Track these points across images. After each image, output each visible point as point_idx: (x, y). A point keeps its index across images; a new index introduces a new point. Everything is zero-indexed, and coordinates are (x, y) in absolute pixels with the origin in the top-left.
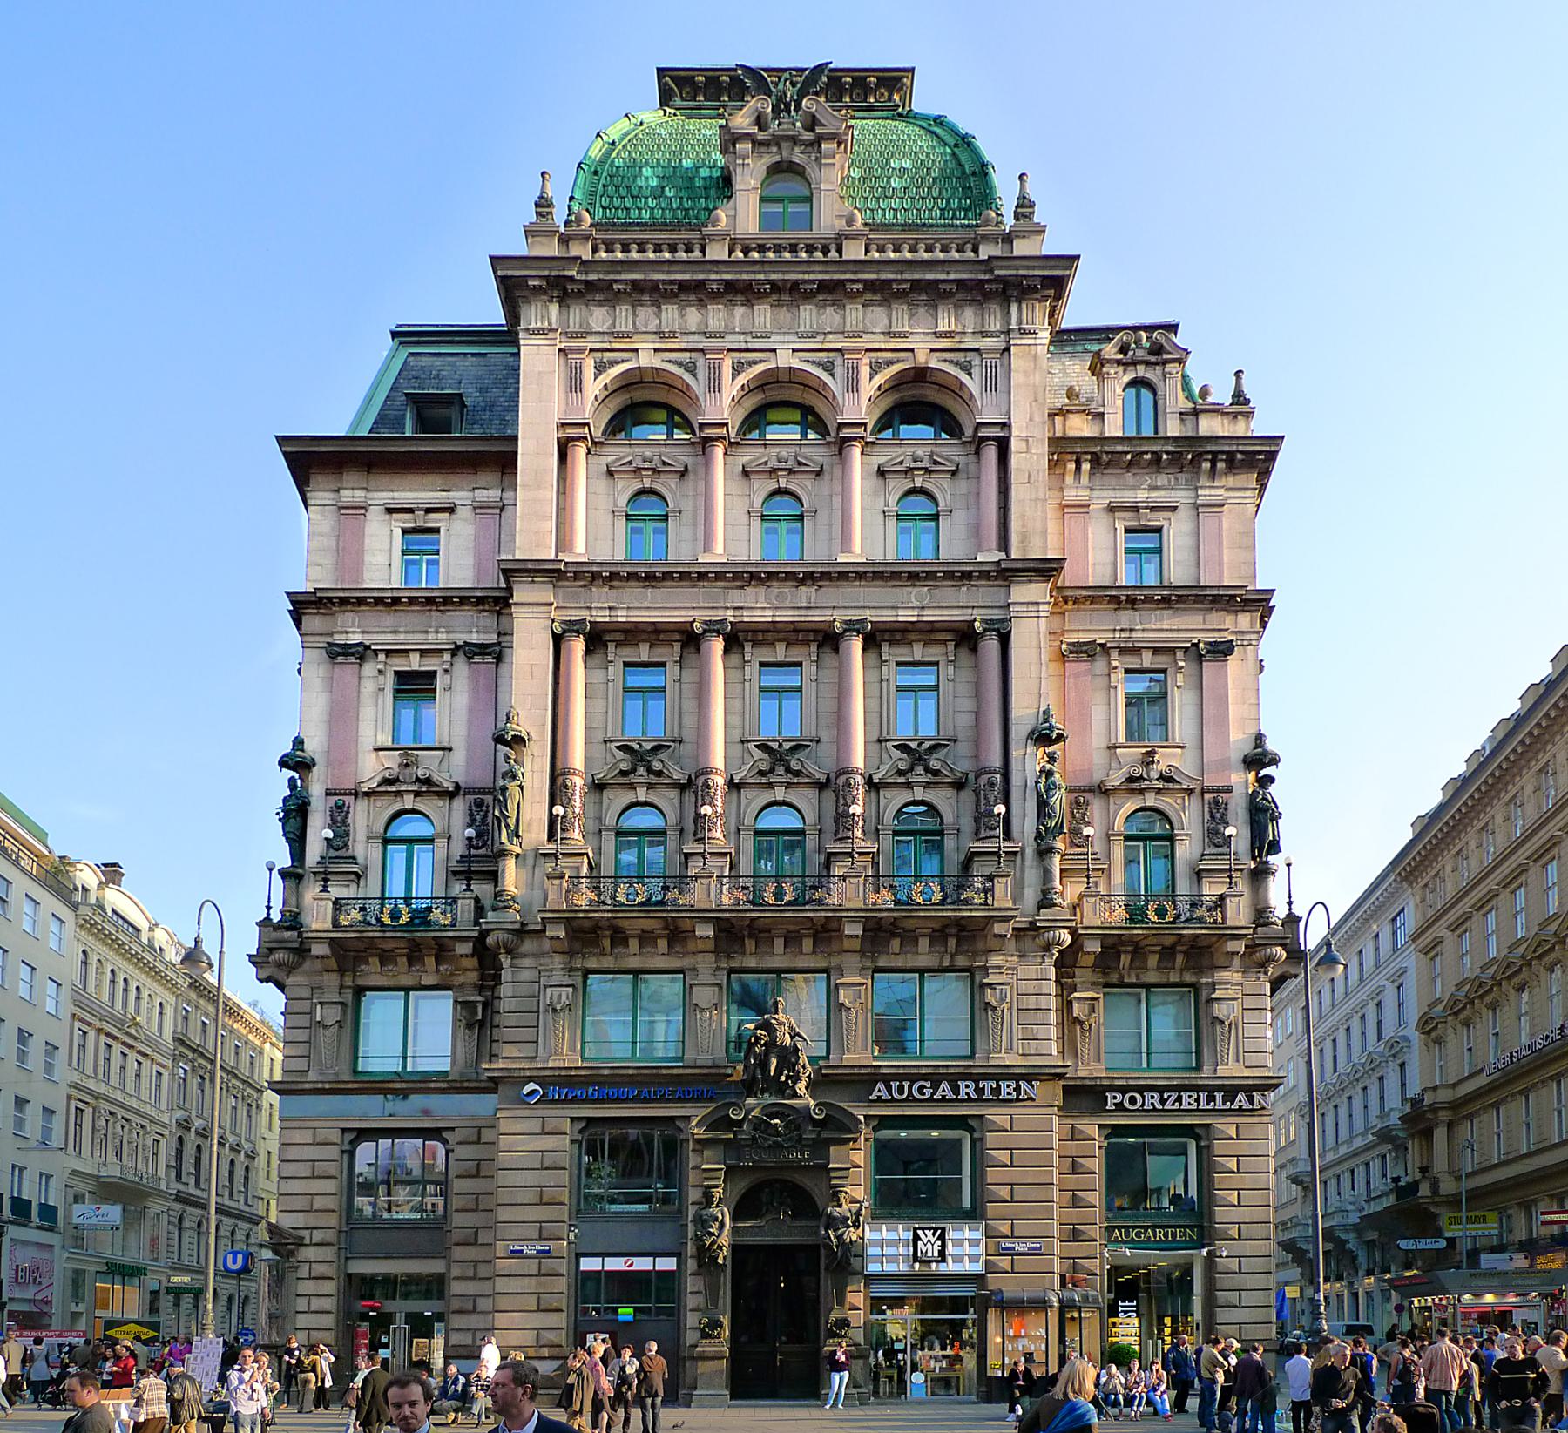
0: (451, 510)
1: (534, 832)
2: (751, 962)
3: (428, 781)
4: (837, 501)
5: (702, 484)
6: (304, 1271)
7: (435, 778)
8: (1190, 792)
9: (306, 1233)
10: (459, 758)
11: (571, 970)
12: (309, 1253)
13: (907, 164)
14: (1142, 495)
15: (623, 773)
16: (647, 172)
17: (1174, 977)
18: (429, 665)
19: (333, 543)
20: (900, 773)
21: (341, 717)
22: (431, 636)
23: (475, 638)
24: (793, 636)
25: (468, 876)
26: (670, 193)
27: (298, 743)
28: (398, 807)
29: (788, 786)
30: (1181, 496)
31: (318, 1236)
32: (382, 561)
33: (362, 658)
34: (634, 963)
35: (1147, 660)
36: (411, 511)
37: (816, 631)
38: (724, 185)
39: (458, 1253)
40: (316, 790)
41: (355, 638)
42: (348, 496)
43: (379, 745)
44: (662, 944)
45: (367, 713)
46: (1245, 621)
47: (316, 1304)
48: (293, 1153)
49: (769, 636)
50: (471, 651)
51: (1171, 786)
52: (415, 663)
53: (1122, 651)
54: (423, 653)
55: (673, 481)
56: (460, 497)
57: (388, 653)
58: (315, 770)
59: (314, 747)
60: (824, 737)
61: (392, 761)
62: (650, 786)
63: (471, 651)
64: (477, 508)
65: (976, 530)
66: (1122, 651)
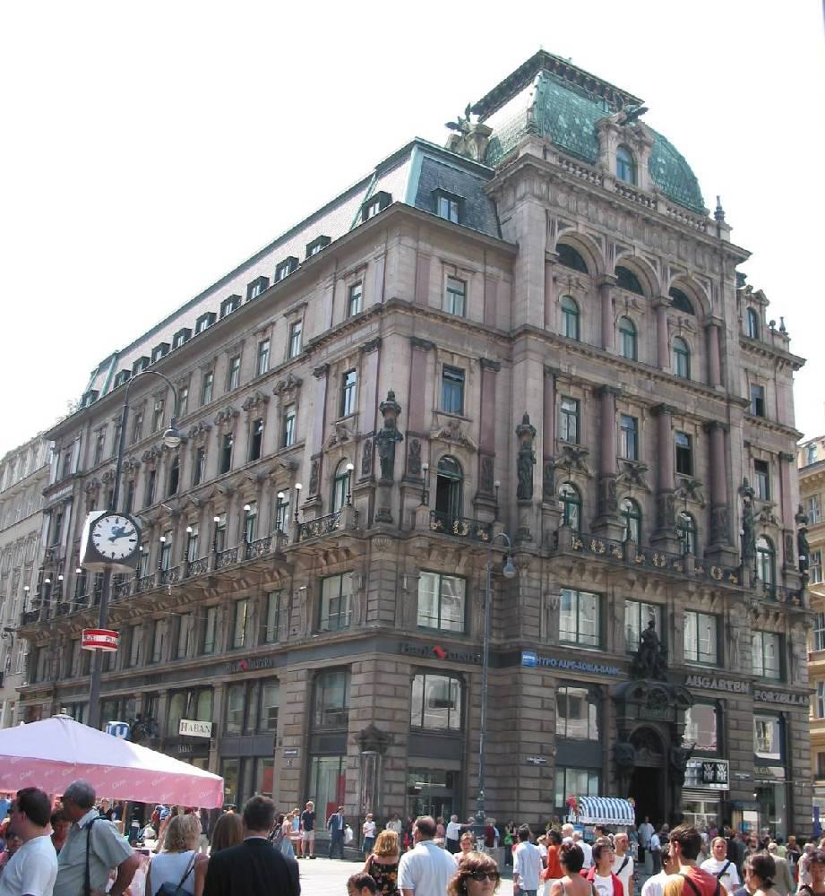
0: (475, 272)
1: (538, 495)
3: (464, 441)
4: (653, 332)
5: (598, 305)
6: (388, 764)
7: (469, 439)
9: (391, 735)
10: (475, 428)
12: (393, 751)
13: (664, 162)
14: (755, 368)
16: (561, 118)
17: (775, 630)
19: (412, 271)
20: (683, 495)
21: (414, 385)
23: (486, 355)
25: (496, 511)
26: (574, 135)
27: (391, 396)
30: (769, 373)
31: (398, 739)
32: (438, 293)
33: (427, 349)
34: (583, 585)
36: (455, 267)
38: (597, 140)
40: (401, 429)
41: (423, 335)
42: (424, 246)
45: (429, 387)
46: (792, 443)
47: (396, 788)
48: (384, 678)
49: (629, 400)
52: (456, 363)
56: (478, 266)
58: (400, 415)
59: (401, 399)
60: (648, 462)
61: (443, 420)
63: (483, 363)
64: (485, 273)
65: (708, 368)
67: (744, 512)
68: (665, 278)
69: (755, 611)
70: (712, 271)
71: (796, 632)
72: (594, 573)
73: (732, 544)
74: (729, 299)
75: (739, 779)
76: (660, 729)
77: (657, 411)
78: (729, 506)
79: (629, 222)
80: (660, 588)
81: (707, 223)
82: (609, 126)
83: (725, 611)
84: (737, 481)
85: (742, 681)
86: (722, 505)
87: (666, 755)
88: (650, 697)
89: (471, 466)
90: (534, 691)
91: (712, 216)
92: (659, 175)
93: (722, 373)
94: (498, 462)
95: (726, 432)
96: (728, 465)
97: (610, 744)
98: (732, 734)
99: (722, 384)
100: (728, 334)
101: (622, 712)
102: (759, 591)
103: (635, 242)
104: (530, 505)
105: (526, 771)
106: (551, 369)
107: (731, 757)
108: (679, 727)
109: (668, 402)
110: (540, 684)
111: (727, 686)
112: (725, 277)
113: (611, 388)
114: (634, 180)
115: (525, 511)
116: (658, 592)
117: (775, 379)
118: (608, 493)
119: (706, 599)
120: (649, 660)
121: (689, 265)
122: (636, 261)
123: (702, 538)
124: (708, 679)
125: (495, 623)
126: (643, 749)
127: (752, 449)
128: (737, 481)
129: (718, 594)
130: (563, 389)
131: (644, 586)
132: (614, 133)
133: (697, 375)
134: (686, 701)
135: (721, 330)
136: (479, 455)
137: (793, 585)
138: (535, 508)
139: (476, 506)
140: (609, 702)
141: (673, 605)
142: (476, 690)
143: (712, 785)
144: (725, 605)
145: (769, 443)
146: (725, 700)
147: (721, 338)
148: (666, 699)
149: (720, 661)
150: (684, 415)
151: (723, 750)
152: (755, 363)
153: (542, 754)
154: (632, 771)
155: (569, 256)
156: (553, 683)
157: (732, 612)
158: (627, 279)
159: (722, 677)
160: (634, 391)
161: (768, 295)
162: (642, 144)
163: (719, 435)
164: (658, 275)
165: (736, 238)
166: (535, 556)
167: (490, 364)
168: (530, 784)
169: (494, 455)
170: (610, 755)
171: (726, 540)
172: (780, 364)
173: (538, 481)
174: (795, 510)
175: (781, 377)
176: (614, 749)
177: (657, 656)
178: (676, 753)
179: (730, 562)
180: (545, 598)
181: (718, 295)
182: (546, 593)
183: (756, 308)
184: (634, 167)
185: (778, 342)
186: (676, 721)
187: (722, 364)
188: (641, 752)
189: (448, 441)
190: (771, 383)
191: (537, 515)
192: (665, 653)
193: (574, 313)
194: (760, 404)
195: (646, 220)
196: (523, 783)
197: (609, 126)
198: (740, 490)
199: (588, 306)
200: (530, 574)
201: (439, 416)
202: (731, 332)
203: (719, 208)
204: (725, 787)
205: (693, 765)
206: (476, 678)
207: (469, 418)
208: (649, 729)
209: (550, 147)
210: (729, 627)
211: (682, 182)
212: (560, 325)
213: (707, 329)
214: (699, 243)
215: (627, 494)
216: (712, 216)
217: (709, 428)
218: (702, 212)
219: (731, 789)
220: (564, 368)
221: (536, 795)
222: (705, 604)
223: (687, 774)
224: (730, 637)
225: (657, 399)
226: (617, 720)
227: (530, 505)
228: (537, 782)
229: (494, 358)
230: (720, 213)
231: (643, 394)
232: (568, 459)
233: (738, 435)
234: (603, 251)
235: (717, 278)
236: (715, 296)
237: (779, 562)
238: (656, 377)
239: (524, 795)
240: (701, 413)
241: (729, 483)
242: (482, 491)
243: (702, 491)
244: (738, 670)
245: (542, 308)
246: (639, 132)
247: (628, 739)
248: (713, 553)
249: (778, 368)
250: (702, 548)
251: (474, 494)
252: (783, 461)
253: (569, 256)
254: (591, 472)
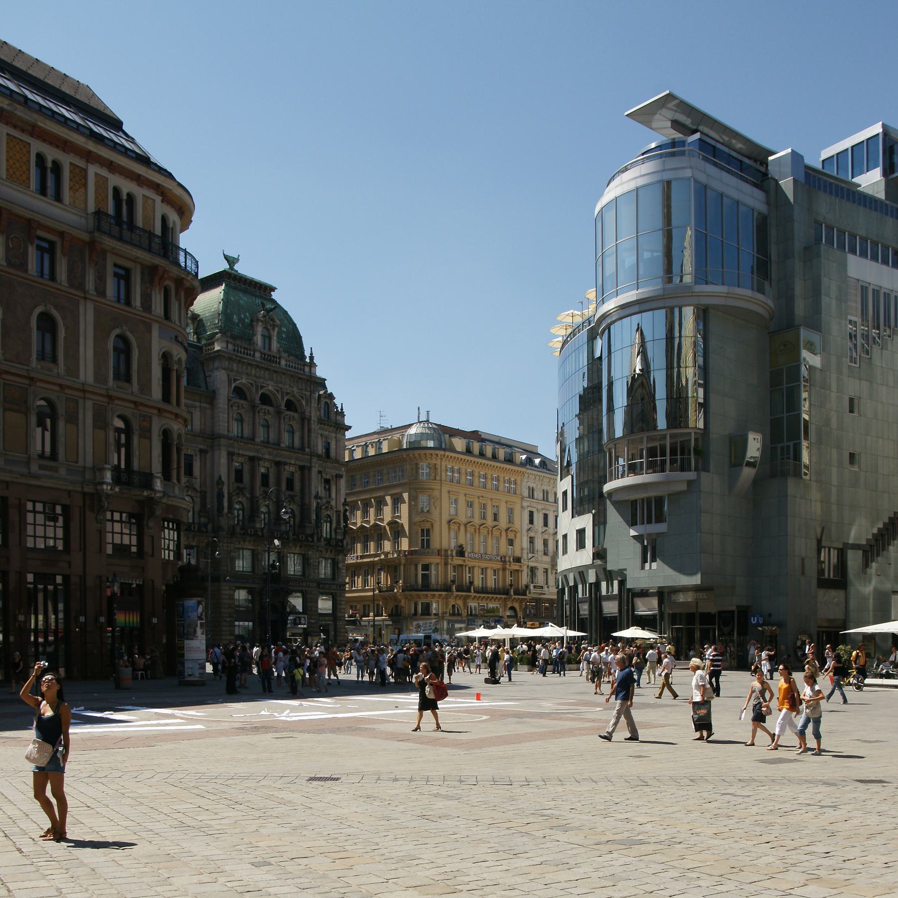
68: (283, 398)
70: (306, 390)
71: (340, 557)
72: (250, 542)
73: (310, 523)
74: (314, 404)
77: (278, 464)
78: (310, 504)
79: (267, 372)
81: (305, 364)
82: (258, 320)
84: (314, 493)
90: (227, 592)
91: (308, 360)
92: (283, 339)
93: (309, 441)
94: (208, 495)
96: (310, 486)
99: (309, 447)
102: (323, 543)
103: (269, 382)
109: (283, 460)
114: (270, 350)
119: (298, 548)
121: (295, 389)
122: (270, 391)
123: (298, 519)
128: (314, 493)
130: (235, 458)
132: (260, 324)
133: (297, 443)
134: (289, 593)
135: (309, 420)
137: (340, 537)
145: (330, 473)
147: (309, 424)
149: (304, 574)
155: (239, 392)
158: (266, 399)
160: (267, 457)
162: (274, 326)
163: (307, 472)
164: (280, 397)
165: (320, 372)
174: (342, 500)
179: (309, 532)
181: (309, 402)
184: (270, 338)
185: (339, 418)
193: (241, 420)
194: (328, 450)
195: (275, 372)
197: (258, 320)
199: (247, 418)
203: (311, 354)
209: (230, 340)
210: (308, 559)
211: (293, 339)
212: (235, 429)
213: (303, 419)
214: (300, 378)
216: (308, 360)
217: (302, 468)
218: (304, 357)
222: (297, 550)
225: (278, 459)
230: (312, 358)
231: (271, 458)
233: (314, 471)
234: (254, 391)
235: (308, 393)
236: (307, 404)
237: (334, 526)
240: (297, 463)
241: (310, 493)
243: (297, 499)
246: (273, 320)
248: (302, 525)
250: (297, 524)
253: (239, 392)
254: (248, 496)
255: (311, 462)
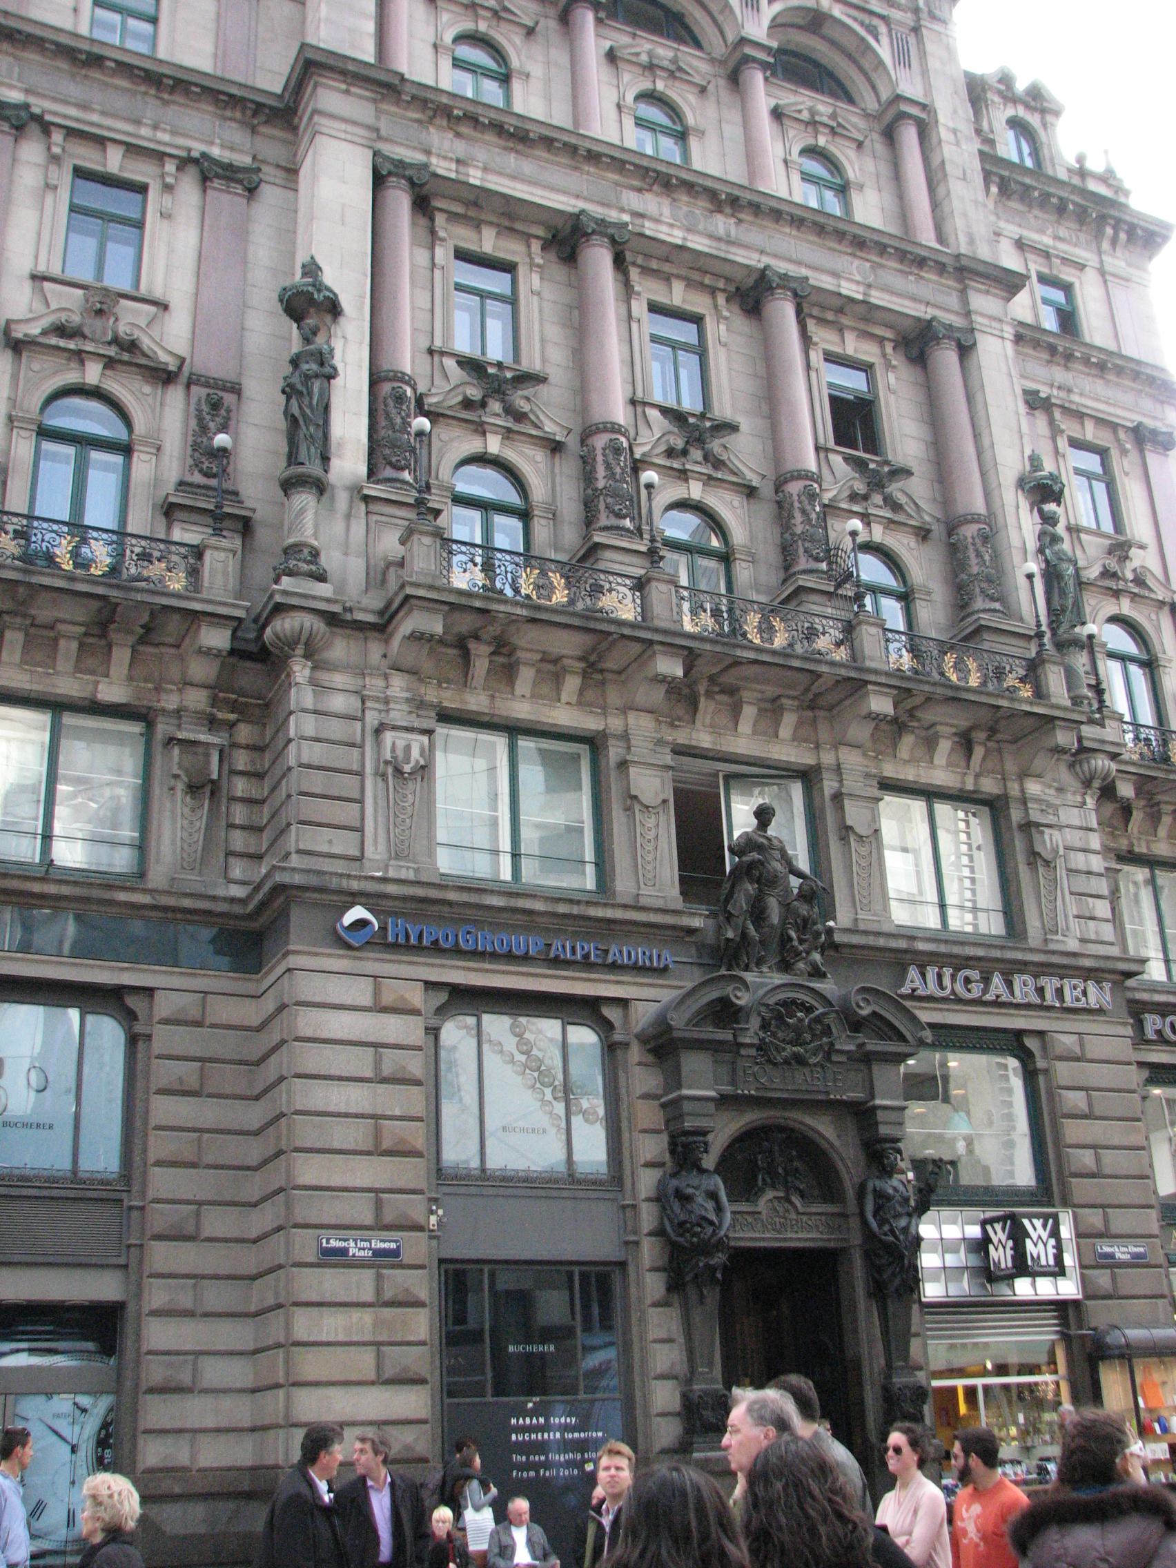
1: (349, 458)
2: (704, 740)
3: (132, 346)
7: (146, 343)
8: (1162, 603)
11: (419, 705)
14: (1046, 240)
15: (467, 404)
18: (139, 171)
20: (854, 497)
22: (144, 131)
23: (216, 152)
24: (696, 276)
28: (71, 377)
29: (709, 480)
30: (1083, 254)
34: (521, 709)
35: (1090, 432)
37: (728, 280)
39: (162, 1255)
43: (42, 268)
44: (572, 684)
50: (209, 172)
51: (1147, 593)
52: (114, 162)
53: (1066, 410)
54: (133, 150)
55: (518, 39)
57: (71, 133)
61: (67, 303)
62: (508, 434)
66: (1066, 410)
67: (1041, 535)
69: (1108, 792)
75: (1109, 1262)
76: (824, 1128)
80: (789, 721)
83: (1014, 789)
85: (1089, 974)
86: (974, 519)
87: (852, 1206)
88: (765, 1026)
89: (166, 418)
95: (965, 350)
97: (647, 1181)
98: (1074, 1131)
100: (944, 134)
101: (674, 1079)
104: (320, 487)
105: (331, 1283)
106: (401, 164)
107: (1077, 1197)
108: (881, 1116)
109: (782, 267)
110: (367, 1001)
111: (1040, 991)
112: (924, 15)
113: (602, 222)
115: (304, 499)
116: (785, 731)
117: (1102, 272)
118: (601, 472)
119: (945, 746)
120: (758, 913)
124: (975, 975)
125: (239, 841)
126: (770, 1194)
127: (1057, 414)
129: (980, 736)
131: (735, 713)
135: (925, 130)
136: (188, 386)
138: (342, 499)
139: (169, 511)
140: (635, 1053)
141: (838, 769)
142: (164, 1039)
143: (1023, 1288)
144: (1010, 766)
146: (1041, 1034)
148: (827, 1031)
150: (840, 311)
151: (1050, 1189)
152: (1042, 231)
153: (381, 1226)
154: (720, 1258)
156: (416, 996)
157: (1033, 788)
159: (1023, 967)
161: (1056, 90)
163: (947, 358)
166: (332, 619)
167: (229, 173)
168: (332, 1325)
169: (236, 389)
170: (648, 1217)
171: (997, 606)
172: (1109, 231)
173: (349, 424)
175: (1116, 262)
176: (659, 1198)
177: (786, 907)
178: (879, 1195)
180: (378, 743)
182: (379, 731)
183: (1034, 120)
186: (873, 1098)
187: (935, 205)
188: (762, 1204)
189: (72, 345)
190: (1091, 276)
191: (348, 517)
192: (817, 895)
196: (304, 1325)
198: (1021, 483)
200: (323, 676)
201: (47, 285)
202: (955, 132)
204: (1068, 1288)
205: (952, 1232)
206: (164, 1005)
207: (158, 294)
208: (781, 1129)
215: (676, 492)
219: (1087, 1296)
220: (443, 168)
221: (364, 1363)
223: (928, 1260)
224: (1034, 856)
226: (664, 1106)
227: (320, 487)
228: (365, 1318)
229: (245, 160)
231: (699, 243)
232: (474, 393)
233: (995, 354)
236: (902, 58)
238: (734, 202)
239: (311, 1365)
242: (198, 478)
244: (1072, 945)
245: (370, 27)
247: (709, 1161)
249: (1106, 245)
251: (170, 487)
252: (1148, 446)
255: (968, 314)
